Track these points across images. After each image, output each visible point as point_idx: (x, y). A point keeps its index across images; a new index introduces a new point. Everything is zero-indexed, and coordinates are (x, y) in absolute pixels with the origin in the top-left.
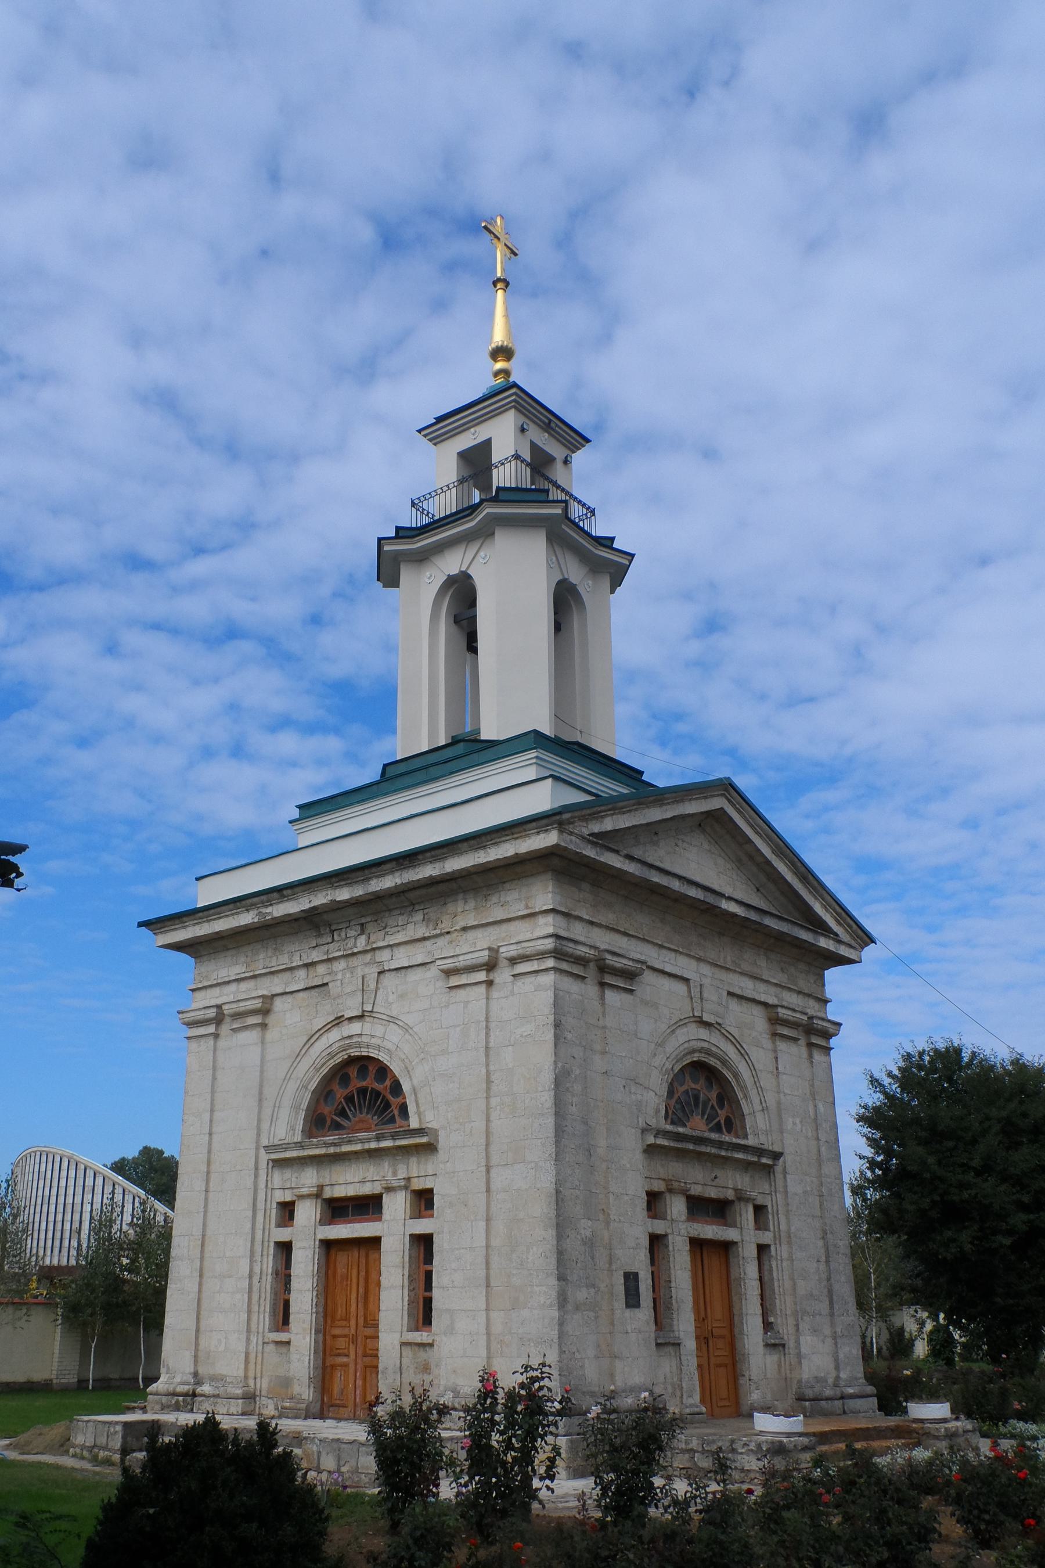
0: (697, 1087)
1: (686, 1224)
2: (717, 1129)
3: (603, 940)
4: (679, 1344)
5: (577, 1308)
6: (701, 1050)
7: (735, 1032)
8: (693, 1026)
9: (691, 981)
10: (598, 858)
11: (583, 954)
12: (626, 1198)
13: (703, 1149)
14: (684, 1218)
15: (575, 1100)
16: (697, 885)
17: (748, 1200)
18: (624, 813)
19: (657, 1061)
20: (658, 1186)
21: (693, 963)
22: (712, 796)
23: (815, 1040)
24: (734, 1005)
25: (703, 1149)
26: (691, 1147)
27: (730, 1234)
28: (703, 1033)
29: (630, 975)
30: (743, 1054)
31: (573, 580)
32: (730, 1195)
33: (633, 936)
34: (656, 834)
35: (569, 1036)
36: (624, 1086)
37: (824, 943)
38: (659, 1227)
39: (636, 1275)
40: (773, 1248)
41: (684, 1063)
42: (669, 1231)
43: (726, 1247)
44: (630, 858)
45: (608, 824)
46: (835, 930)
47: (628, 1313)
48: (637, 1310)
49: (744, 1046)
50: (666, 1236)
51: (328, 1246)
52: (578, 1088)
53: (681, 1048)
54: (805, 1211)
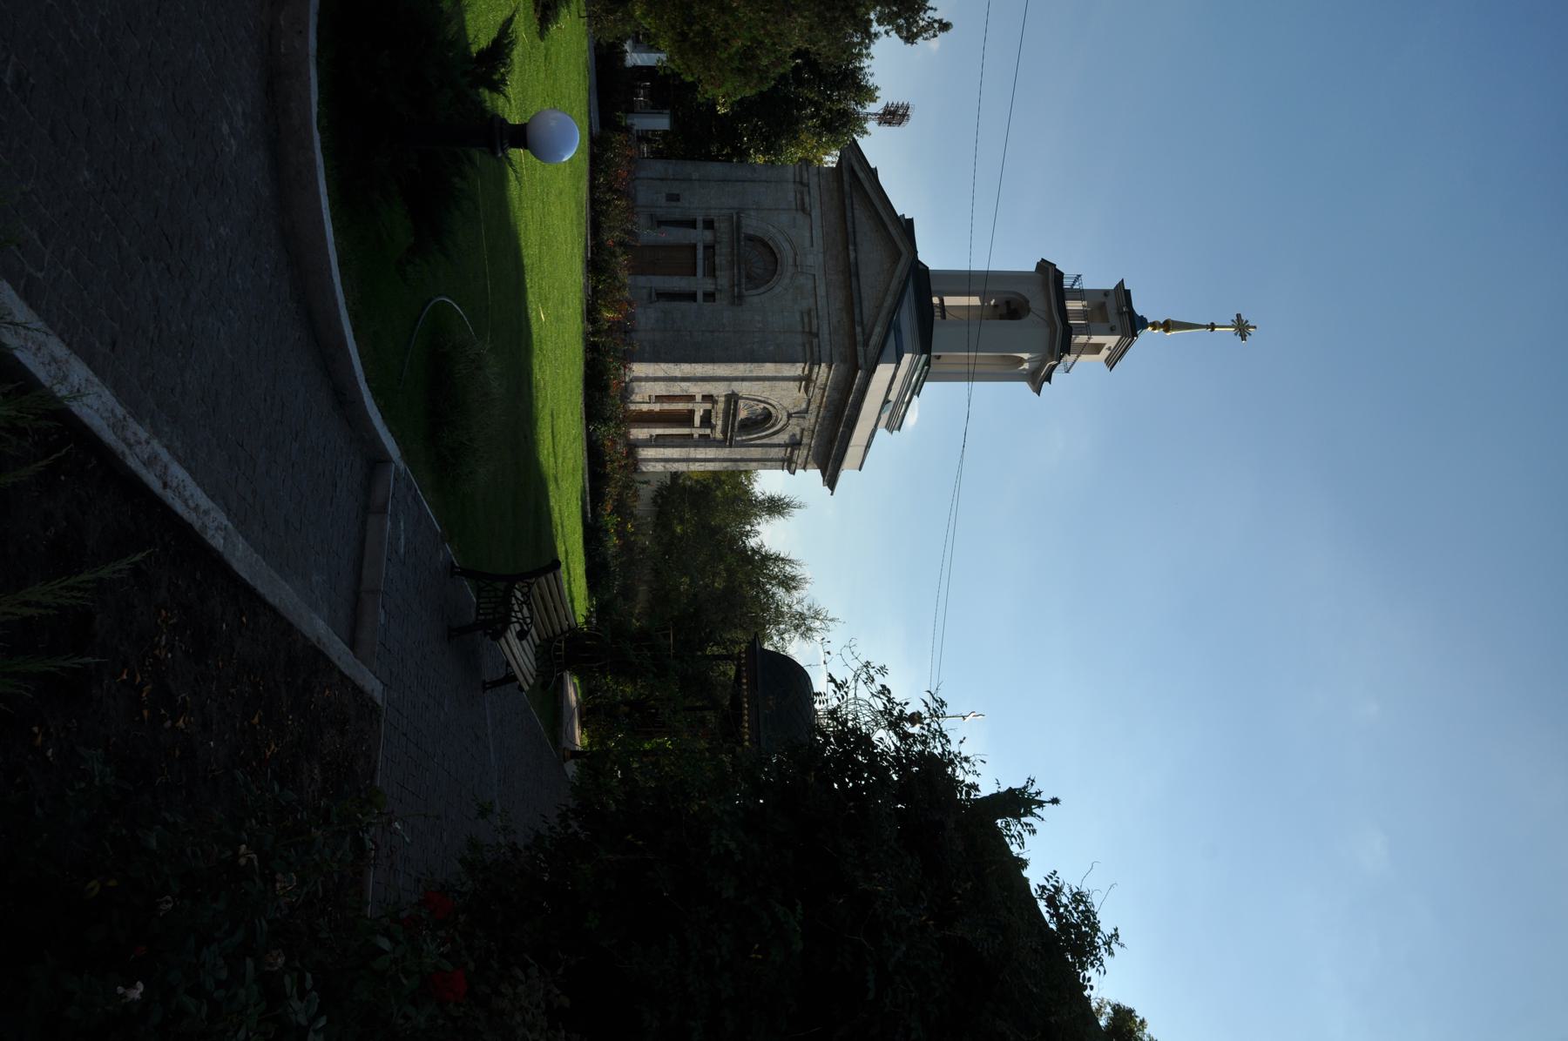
3: (815, 192)
13: (735, 245)
16: (854, 228)
17: (716, 284)
20: (716, 225)
21: (822, 250)
23: (807, 346)
25: (735, 245)
28: (791, 261)
29: (803, 210)
31: (1032, 305)
32: (718, 273)
37: (858, 329)
38: (700, 225)
39: (678, 200)
40: (695, 304)
43: (695, 275)
44: (850, 187)
45: (861, 175)
50: (695, 228)
51: (694, 247)
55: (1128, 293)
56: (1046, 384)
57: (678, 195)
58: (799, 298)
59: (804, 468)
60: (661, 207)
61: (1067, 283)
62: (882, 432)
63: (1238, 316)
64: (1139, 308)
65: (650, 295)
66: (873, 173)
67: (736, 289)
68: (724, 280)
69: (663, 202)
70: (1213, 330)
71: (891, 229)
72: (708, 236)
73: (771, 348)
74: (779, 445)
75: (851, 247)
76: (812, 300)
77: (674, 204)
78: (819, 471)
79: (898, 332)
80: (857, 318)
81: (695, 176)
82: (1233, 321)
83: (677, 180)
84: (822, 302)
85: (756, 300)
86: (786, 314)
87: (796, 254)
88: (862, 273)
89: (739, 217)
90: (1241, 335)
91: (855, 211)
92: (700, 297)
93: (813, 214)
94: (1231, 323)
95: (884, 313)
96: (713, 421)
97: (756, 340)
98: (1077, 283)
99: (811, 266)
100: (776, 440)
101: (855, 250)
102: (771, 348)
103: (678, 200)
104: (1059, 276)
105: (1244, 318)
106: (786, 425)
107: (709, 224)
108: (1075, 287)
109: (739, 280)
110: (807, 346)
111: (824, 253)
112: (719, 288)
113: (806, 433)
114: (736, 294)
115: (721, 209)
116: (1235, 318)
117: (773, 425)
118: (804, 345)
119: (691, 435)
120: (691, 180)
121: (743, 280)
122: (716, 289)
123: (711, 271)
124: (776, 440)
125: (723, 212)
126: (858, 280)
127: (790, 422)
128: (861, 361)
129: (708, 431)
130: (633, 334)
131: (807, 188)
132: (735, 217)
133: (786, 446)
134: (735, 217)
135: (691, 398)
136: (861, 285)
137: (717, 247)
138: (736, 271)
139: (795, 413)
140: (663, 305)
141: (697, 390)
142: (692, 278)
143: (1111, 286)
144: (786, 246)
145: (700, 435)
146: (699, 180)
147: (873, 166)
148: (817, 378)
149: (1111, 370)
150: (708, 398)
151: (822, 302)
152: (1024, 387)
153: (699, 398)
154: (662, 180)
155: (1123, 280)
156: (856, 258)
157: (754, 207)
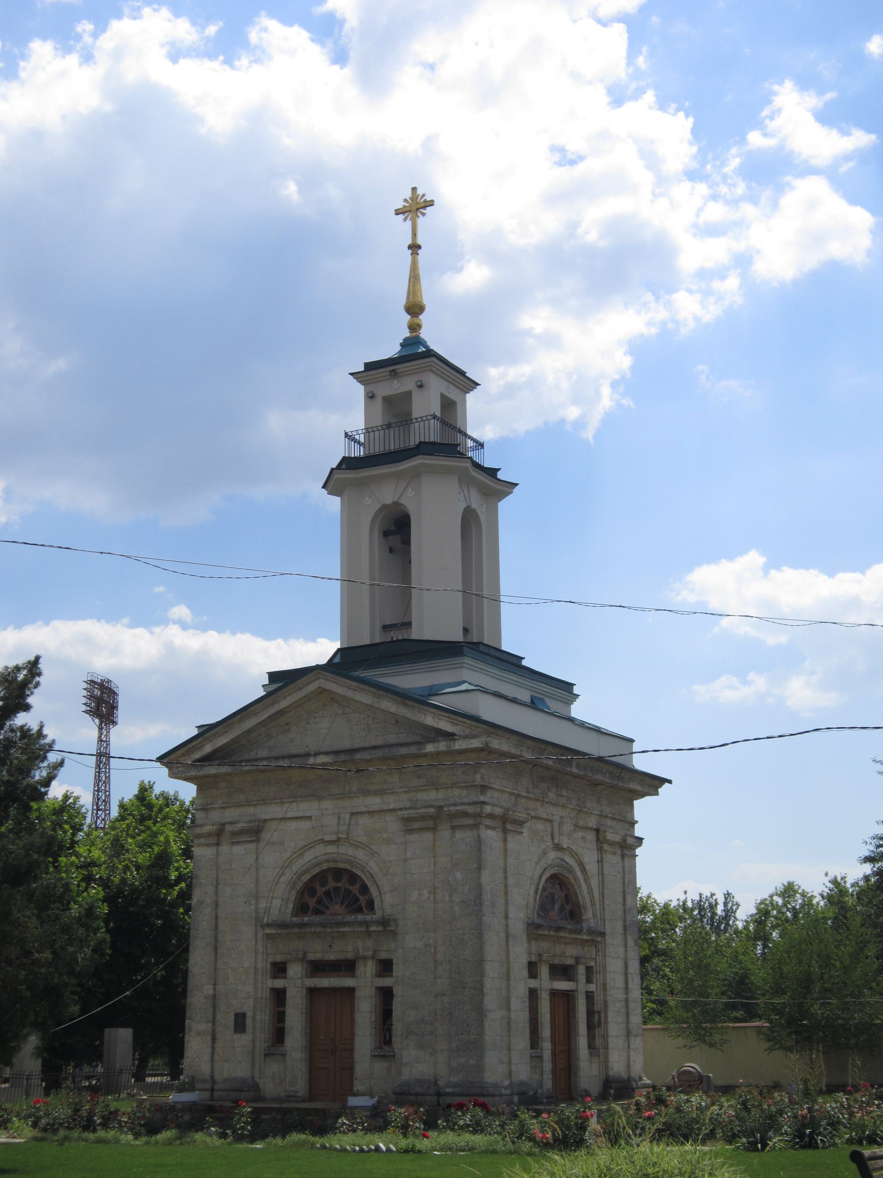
0: (339, 885)
1: (304, 979)
2: (360, 910)
3: (230, 814)
4: (285, 1055)
5: (199, 1033)
6: (327, 861)
7: (364, 839)
8: (322, 845)
9: (313, 818)
10: (198, 774)
11: (208, 831)
12: (241, 969)
14: (299, 976)
15: (205, 918)
17: (365, 958)
18: (221, 736)
19: (284, 879)
20: (279, 958)
21: (315, 804)
22: (309, 683)
24: (364, 820)
26: (296, 930)
27: (348, 982)
28: (331, 849)
30: (373, 854)
31: (389, 501)
32: (350, 956)
33: (258, 804)
34: (287, 724)
35: (203, 881)
36: (245, 902)
38: (279, 983)
39: (243, 1015)
41: (313, 874)
42: (287, 985)
45: (208, 749)
46: (450, 731)
47: (236, 1036)
48: (243, 1034)
49: (373, 847)
52: (208, 910)
53: (309, 864)
54: (424, 959)
55: (370, 366)
56: (500, 475)
57: (237, 1015)
58: (385, 835)
59: (633, 823)
60: (253, 1041)
61: (358, 452)
62: (577, 711)
63: (398, 212)
64: (391, 349)
65: (384, 1057)
66: (206, 731)
67: (373, 928)
68: (364, 946)
69: (245, 1038)
70: (419, 247)
71: (283, 704)
72: (295, 970)
73: (459, 875)
74: (600, 861)
75: (311, 761)
76: (389, 817)
77: (249, 1021)
78: (636, 802)
79: (434, 691)
80: (413, 750)
81: (208, 990)
82: (405, 219)
83: (214, 1017)
84: (391, 802)
85: (388, 899)
86: (409, 855)
87: (322, 841)
88: (347, 745)
89: (269, 925)
90: (425, 207)
91: (259, 756)
92: (386, 982)
93: (267, 817)
94: (409, 223)
95: (403, 711)
96: (569, 961)
97: (447, 898)
98: (357, 437)
99: (339, 818)
100: (592, 867)
101: (316, 754)
102: (459, 875)
103: (243, 1015)
104: (347, 463)
105: (400, 205)
106: (574, 855)
107: (279, 969)
108: (362, 440)
109: (361, 923)
110: (457, 822)
111: (319, 798)
112: (370, 953)
113: (581, 823)
114: (380, 929)
115: (256, 952)
116: (401, 217)
117: (570, 870)
118: (454, 828)
119: (589, 996)
120: (214, 996)
121: (360, 917)
122: (373, 958)
123: (348, 967)
124: (592, 867)
125: (260, 949)
126: (357, 750)
127: (565, 846)
128: (476, 743)
129: (581, 970)
130: (441, 1083)
131: (227, 826)
132: (268, 931)
133: (600, 850)
134: (268, 931)
135: (533, 994)
136: (367, 745)
137: (311, 957)
138: (347, 929)
139: (553, 839)
140: (397, 1040)
141: (521, 986)
142: (358, 994)
143: (359, 390)
144: (309, 856)
145: (589, 981)
146: (215, 985)
147: (195, 732)
148: (502, 807)
149: (478, 385)
150: (532, 970)
151: (391, 802)
152: (505, 506)
153: (533, 983)
154: (214, 1039)
155: (351, 374)
156: (327, 753)
157: (253, 902)
